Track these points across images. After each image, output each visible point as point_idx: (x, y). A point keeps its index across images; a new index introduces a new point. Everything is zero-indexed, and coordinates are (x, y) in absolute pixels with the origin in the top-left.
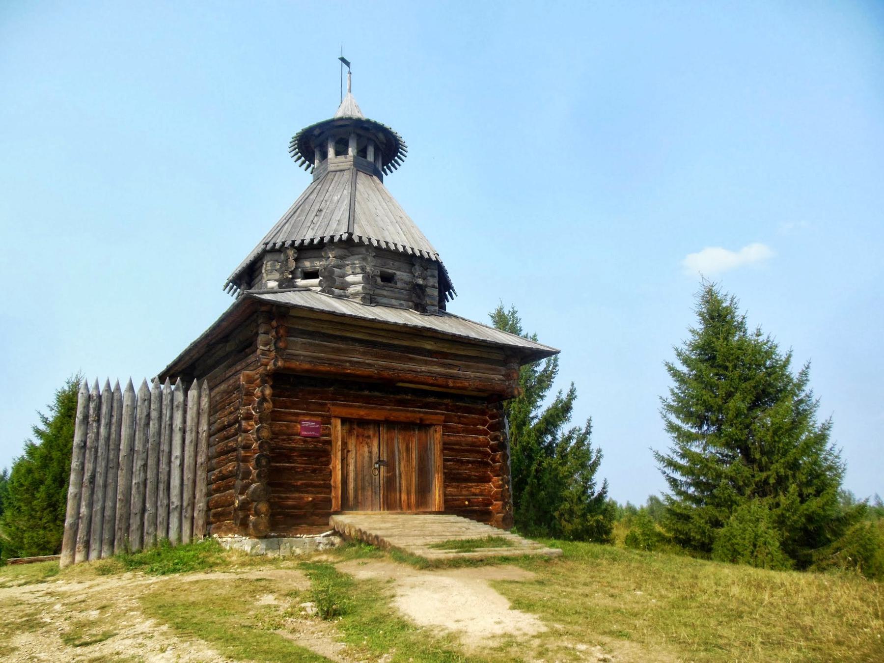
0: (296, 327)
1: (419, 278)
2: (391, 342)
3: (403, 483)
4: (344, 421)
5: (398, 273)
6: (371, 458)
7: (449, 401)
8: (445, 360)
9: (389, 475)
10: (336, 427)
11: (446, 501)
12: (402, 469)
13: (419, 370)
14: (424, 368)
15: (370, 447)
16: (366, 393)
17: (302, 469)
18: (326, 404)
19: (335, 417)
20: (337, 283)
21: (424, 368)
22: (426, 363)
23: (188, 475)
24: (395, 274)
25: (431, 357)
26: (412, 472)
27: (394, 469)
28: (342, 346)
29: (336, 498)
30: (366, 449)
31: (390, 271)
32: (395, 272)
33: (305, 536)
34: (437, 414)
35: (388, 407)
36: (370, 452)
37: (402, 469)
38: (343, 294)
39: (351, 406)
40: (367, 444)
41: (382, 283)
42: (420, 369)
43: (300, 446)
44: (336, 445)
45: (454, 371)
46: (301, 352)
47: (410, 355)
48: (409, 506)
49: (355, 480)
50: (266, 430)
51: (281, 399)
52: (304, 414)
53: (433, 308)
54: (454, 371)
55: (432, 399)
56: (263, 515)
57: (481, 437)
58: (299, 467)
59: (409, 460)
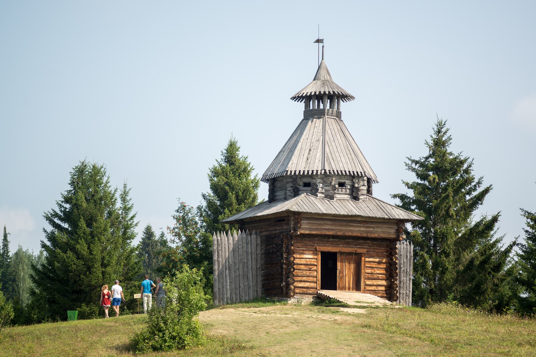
0: (304, 216)
2: (343, 219)
3: (347, 279)
8: (367, 225)
12: (347, 273)
18: (315, 245)
21: (357, 229)
22: (357, 226)
23: (254, 273)
24: (345, 182)
28: (322, 223)
32: (345, 181)
33: (307, 299)
34: (363, 248)
37: (347, 273)
39: (325, 246)
48: (349, 289)
54: (372, 229)
55: (361, 241)
59: (349, 269)
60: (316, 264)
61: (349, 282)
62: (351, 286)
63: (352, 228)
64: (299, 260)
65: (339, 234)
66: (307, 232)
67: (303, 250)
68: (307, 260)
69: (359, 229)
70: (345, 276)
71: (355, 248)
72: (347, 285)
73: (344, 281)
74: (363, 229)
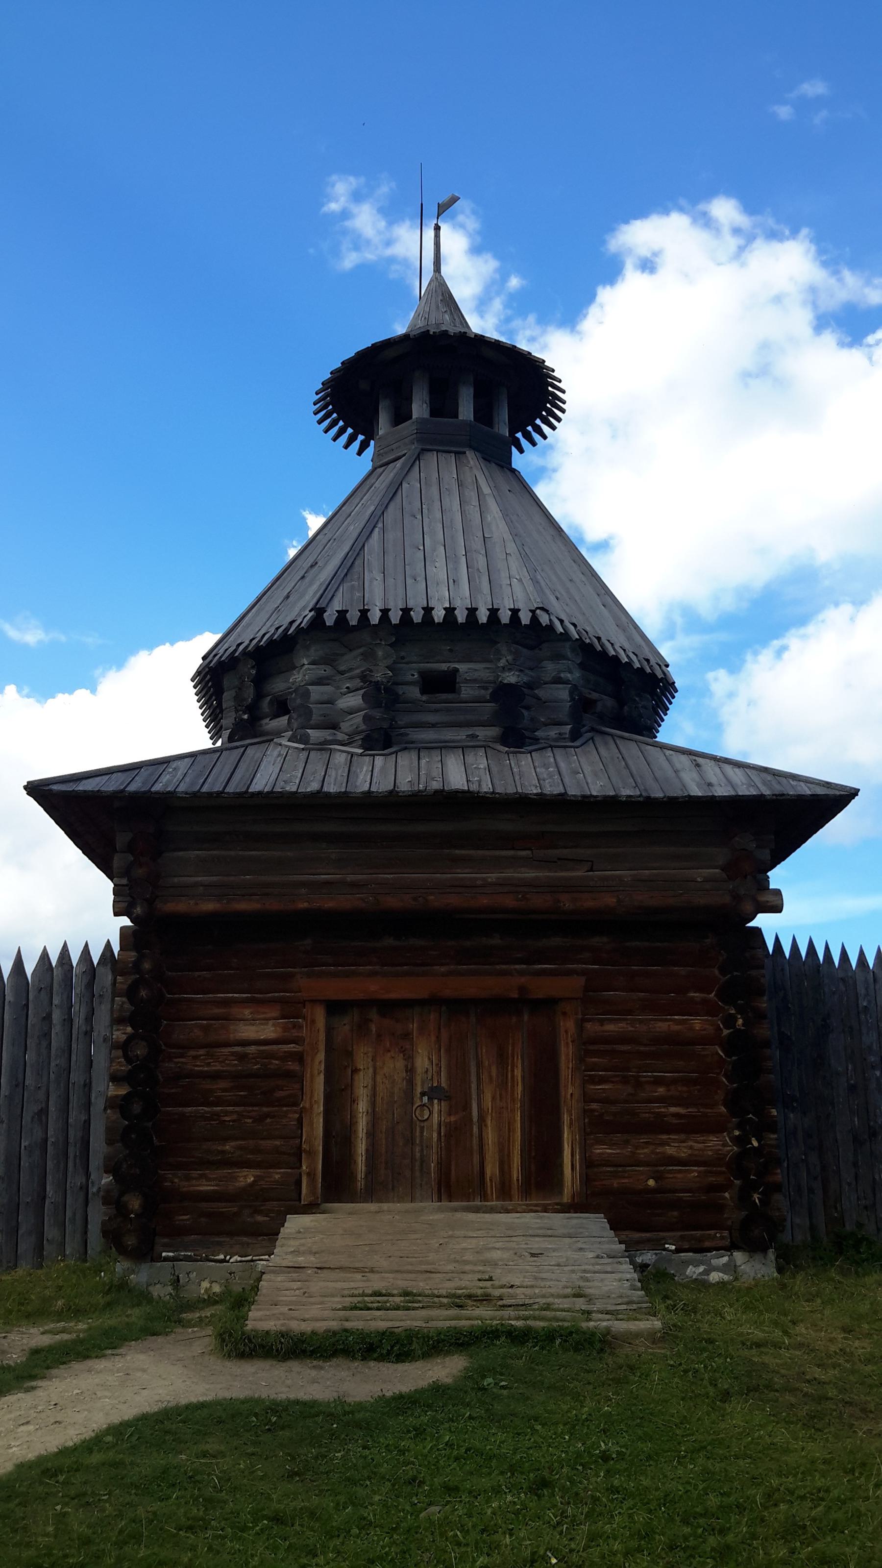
1: (510, 670)
3: (490, 1136)
4: (335, 1008)
5: (462, 667)
6: (411, 1082)
7: (605, 939)
9: (453, 1119)
10: (313, 1022)
11: (587, 1180)
12: (488, 1103)
13: (479, 883)
14: (492, 877)
15: (409, 1058)
16: (389, 941)
17: (235, 1117)
19: (314, 1001)
20: (314, 717)
21: (492, 877)
24: (456, 670)
25: (513, 849)
26: (513, 1111)
27: (467, 1107)
29: (311, 1175)
30: (400, 1063)
31: (444, 667)
34: (569, 973)
35: (443, 969)
36: (410, 1070)
37: (488, 1103)
38: (330, 738)
40: (403, 1051)
41: (424, 698)
42: (484, 879)
43: (233, 1069)
44: (313, 1060)
45: (579, 873)
46: (200, 879)
47: (457, 852)
48: (504, 1192)
49: (371, 1134)
50: (145, 1044)
51: (197, 974)
52: (243, 1001)
53: (553, 732)
54: (579, 873)
56: (132, 1216)
57: (697, 1023)
58: (227, 1113)
60: (293, 1066)
61: (501, 1151)
62: (516, 1173)
63: (464, 874)
64: (202, 1052)
65: (393, 902)
66: (209, 906)
67: (226, 1003)
68: (252, 1049)
69: (509, 874)
70: (482, 1119)
71: (521, 973)
72: (491, 1169)
73: (476, 1147)
74: (530, 874)
